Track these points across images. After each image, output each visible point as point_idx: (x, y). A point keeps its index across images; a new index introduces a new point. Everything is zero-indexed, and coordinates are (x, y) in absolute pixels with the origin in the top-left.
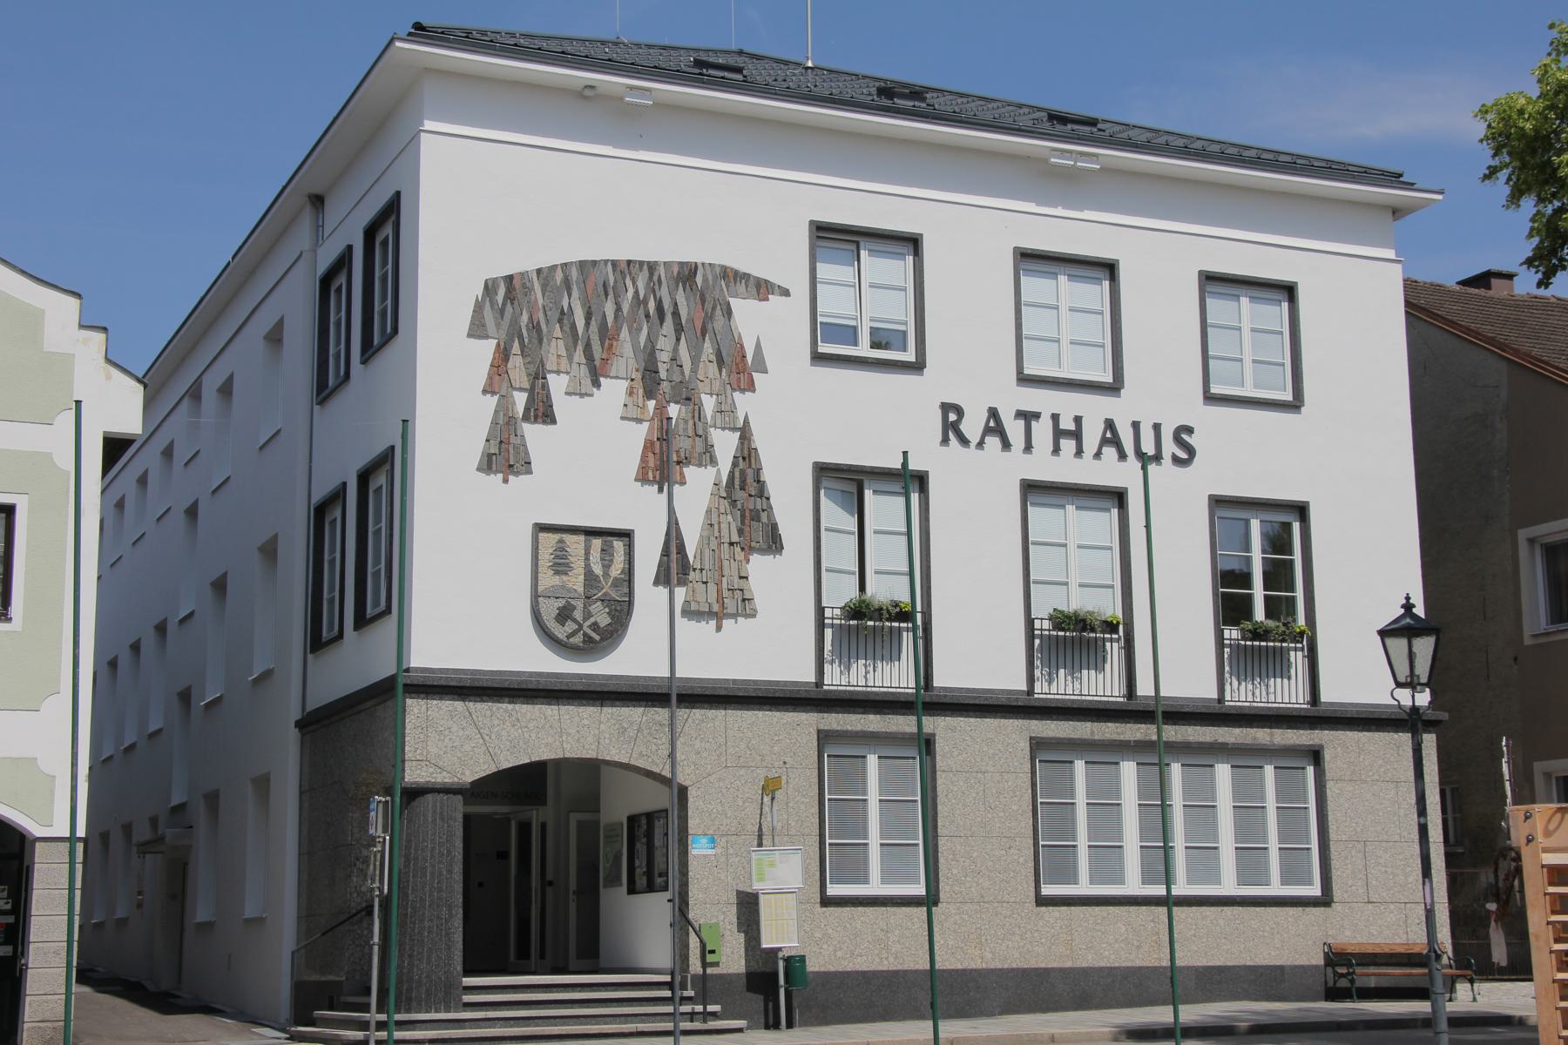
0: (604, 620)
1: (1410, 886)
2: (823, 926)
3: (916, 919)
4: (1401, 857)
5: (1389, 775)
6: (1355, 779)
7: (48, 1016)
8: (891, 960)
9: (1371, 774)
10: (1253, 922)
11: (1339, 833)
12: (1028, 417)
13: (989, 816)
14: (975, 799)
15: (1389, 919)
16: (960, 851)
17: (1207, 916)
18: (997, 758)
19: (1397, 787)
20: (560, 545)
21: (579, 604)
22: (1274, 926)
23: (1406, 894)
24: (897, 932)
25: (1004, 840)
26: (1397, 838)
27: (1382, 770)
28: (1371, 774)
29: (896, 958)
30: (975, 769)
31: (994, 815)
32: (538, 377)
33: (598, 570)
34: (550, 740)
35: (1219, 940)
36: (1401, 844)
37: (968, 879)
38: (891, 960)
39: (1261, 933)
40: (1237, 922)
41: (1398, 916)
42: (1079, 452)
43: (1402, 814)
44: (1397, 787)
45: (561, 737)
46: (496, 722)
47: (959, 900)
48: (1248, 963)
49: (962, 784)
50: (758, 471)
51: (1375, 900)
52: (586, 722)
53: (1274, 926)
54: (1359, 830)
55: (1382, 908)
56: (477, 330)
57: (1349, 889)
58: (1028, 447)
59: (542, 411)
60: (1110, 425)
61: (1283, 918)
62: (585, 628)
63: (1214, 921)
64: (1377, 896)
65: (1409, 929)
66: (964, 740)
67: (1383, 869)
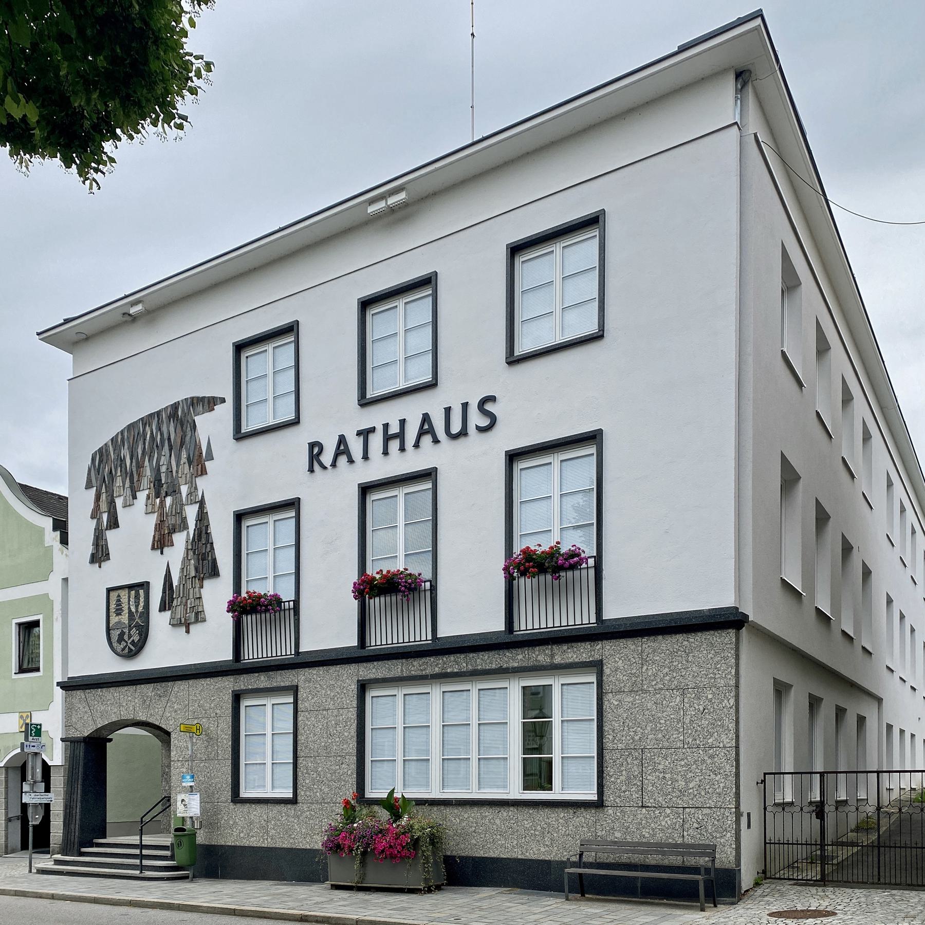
0: (136, 638)
1: (691, 791)
2: (234, 817)
3: (284, 814)
4: (683, 763)
5: (676, 682)
6: (635, 689)
8: (269, 840)
9: (654, 683)
10: (526, 822)
11: (616, 741)
12: (365, 434)
13: (330, 741)
14: (321, 729)
15: (663, 823)
17: (486, 817)
18: (336, 699)
19: (683, 694)
20: (118, 598)
21: (126, 630)
24: (273, 822)
25: (339, 758)
26: (679, 744)
28: (654, 683)
29: (272, 839)
30: (322, 708)
31: (333, 740)
32: (112, 504)
33: (133, 610)
34: (116, 710)
35: (495, 837)
37: (316, 787)
38: (269, 840)
39: (532, 832)
41: (674, 821)
42: (402, 449)
43: (687, 721)
44: (683, 694)
45: (120, 708)
46: (96, 703)
48: (520, 857)
49: (313, 719)
50: (207, 527)
51: (650, 805)
52: (130, 698)
54: (637, 738)
56: (89, 486)
57: (622, 794)
58: (366, 457)
59: (114, 523)
60: (426, 418)
61: (554, 819)
62: (129, 644)
65: (685, 833)
66: (316, 688)
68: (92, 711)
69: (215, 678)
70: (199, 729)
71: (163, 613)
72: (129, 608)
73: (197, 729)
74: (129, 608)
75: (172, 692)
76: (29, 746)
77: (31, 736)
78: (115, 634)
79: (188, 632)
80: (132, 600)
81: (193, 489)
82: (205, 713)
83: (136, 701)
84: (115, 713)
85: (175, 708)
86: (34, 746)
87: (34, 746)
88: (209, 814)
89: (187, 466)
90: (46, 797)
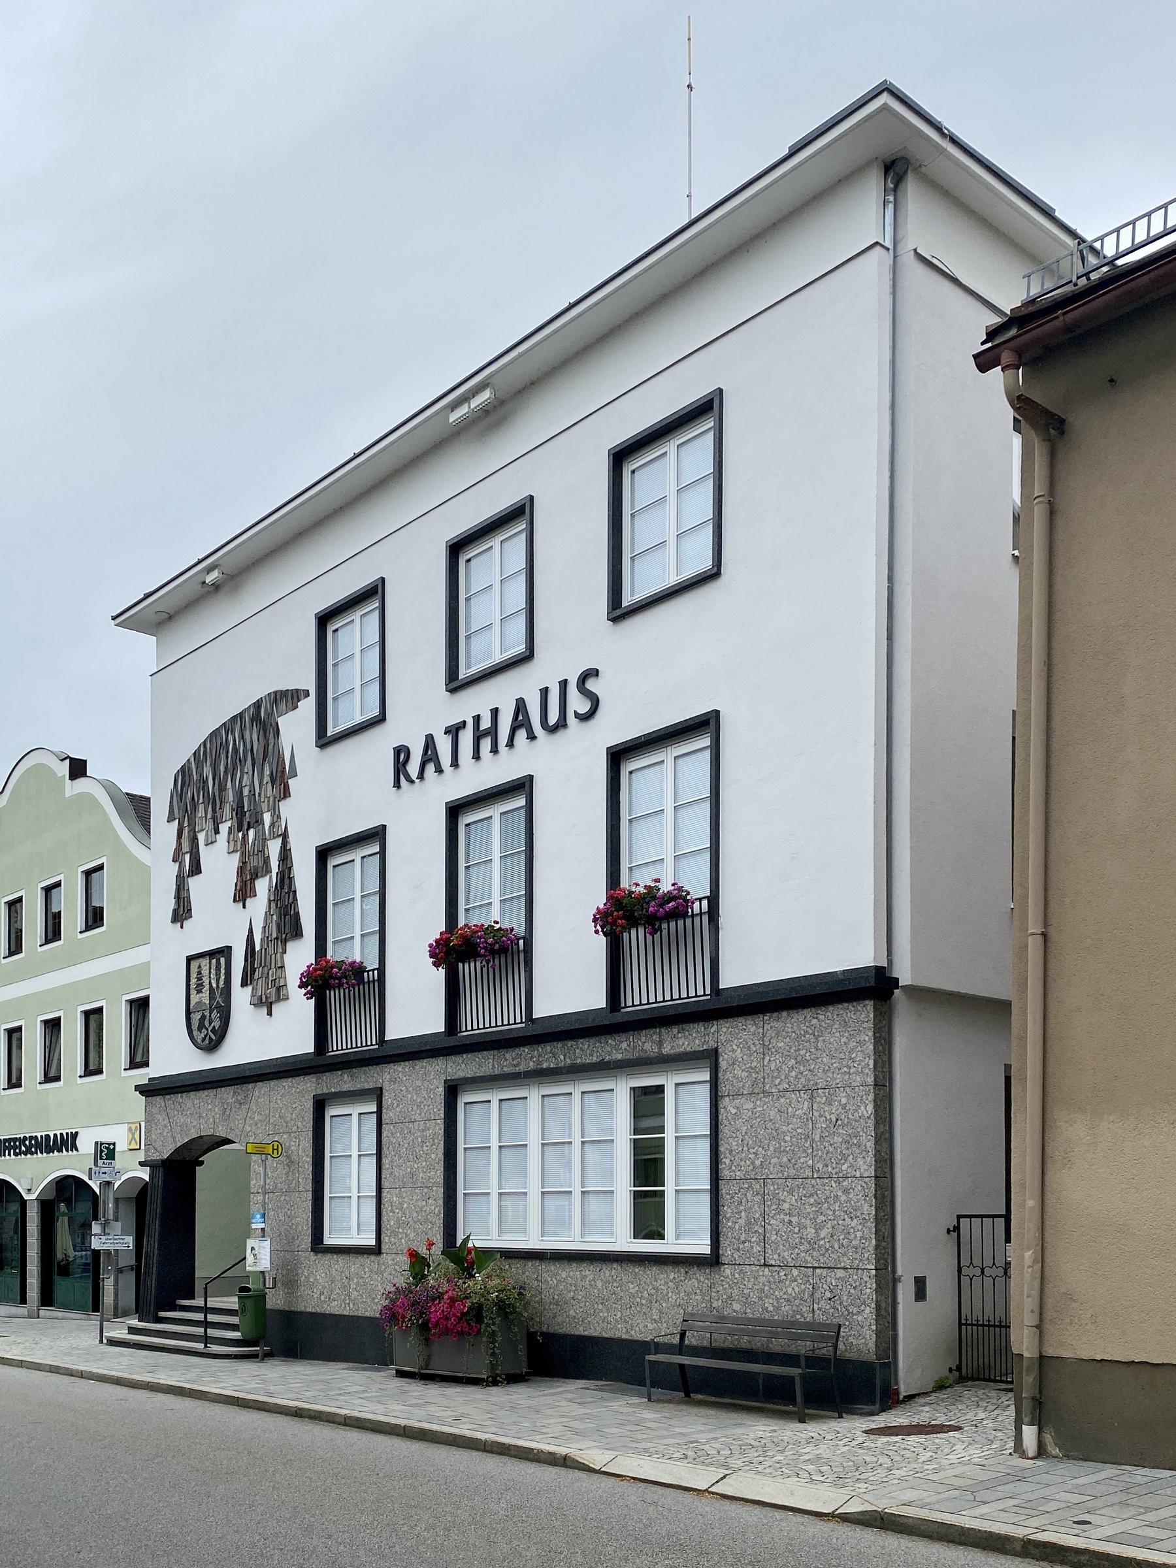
0: (217, 1024)
1: (822, 1242)
2: (314, 1272)
3: (367, 1269)
4: (812, 1200)
5: (803, 1080)
6: (756, 1091)
8: (351, 1305)
9: (777, 1081)
10: (631, 1286)
11: (733, 1168)
12: (454, 731)
13: (416, 1166)
14: (406, 1149)
15: (790, 1290)
16: (395, 1203)
17: (586, 1276)
18: (422, 1106)
19: (812, 1098)
20: (199, 970)
21: (207, 1014)
22: (653, 1291)
23: (815, 1254)
24: (355, 1281)
25: (426, 1190)
26: (808, 1173)
27: (793, 1074)
28: (777, 1081)
29: (354, 1304)
30: (407, 1120)
31: (419, 1165)
32: (194, 841)
33: (214, 985)
34: (195, 1123)
35: (596, 1306)
36: (813, 1181)
37: (401, 1230)
38: (351, 1305)
39: (638, 1300)
40: (615, 1284)
41: (803, 1287)
42: (495, 750)
43: (817, 1139)
44: (812, 1098)
45: (200, 1120)
46: (176, 1113)
47: (394, 1251)
48: (624, 1336)
49: (398, 1135)
50: (290, 869)
51: (773, 1263)
52: (210, 1107)
53: (653, 1291)
54: (758, 1163)
55: (782, 1274)
56: (170, 819)
57: (741, 1246)
58: (455, 763)
59: (196, 869)
60: (521, 706)
61: (663, 1282)
62: (209, 1032)
63: (593, 1282)
64: (776, 1256)
65: (816, 1306)
66: (401, 1090)
67: (787, 1218)
68: (172, 1124)
69: (297, 1078)
70: (277, 1149)
71: (245, 988)
72: (210, 982)
73: (273, 1149)
74: (210, 982)
75: (253, 1098)
76: (99, 1172)
77: (101, 1159)
78: (196, 1018)
79: (270, 1014)
80: (213, 971)
81: (277, 816)
82: (287, 1126)
83: (216, 1110)
84: (194, 1127)
85: (256, 1119)
86: (105, 1173)
87: (105, 1173)
88: (289, 1267)
89: (270, 785)
90: (122, 1241)
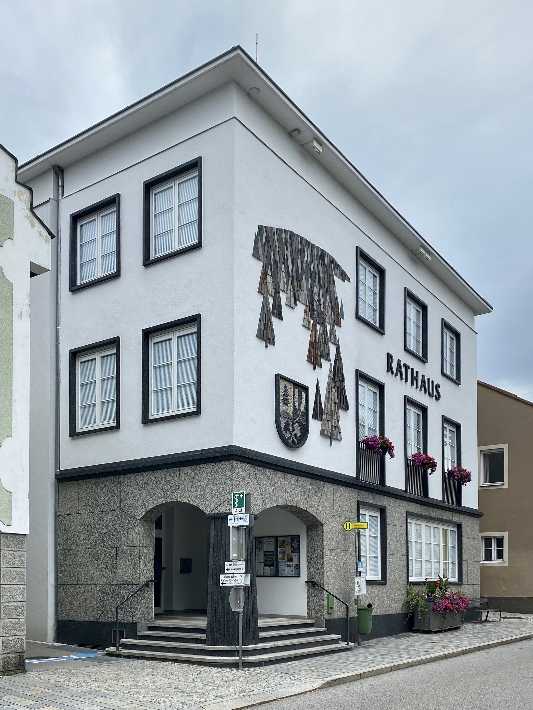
3: (381, 592)
7: (13, 649)
34: (282, 494)
46: (265, 482)
47: (391, 583)
52: (293, 487)
62: (293, 436)
68: (262, 490)
69: (348, 488)
70: (347, 526)
71: (314, 420)
72: (294, 403)
73: (349, 526)
74: (294, 403)
75: (323, 490)
76: (237, 518)
77: (234, 507)
79: (331, 444)
80: (296, 397)
82: (343, 513)
83: (298, 490)
84: (281, 497)
85: (326, 504)
86: (241, 519)
87: (241, 519)
88: (346, 593)
90: (235, 578)
